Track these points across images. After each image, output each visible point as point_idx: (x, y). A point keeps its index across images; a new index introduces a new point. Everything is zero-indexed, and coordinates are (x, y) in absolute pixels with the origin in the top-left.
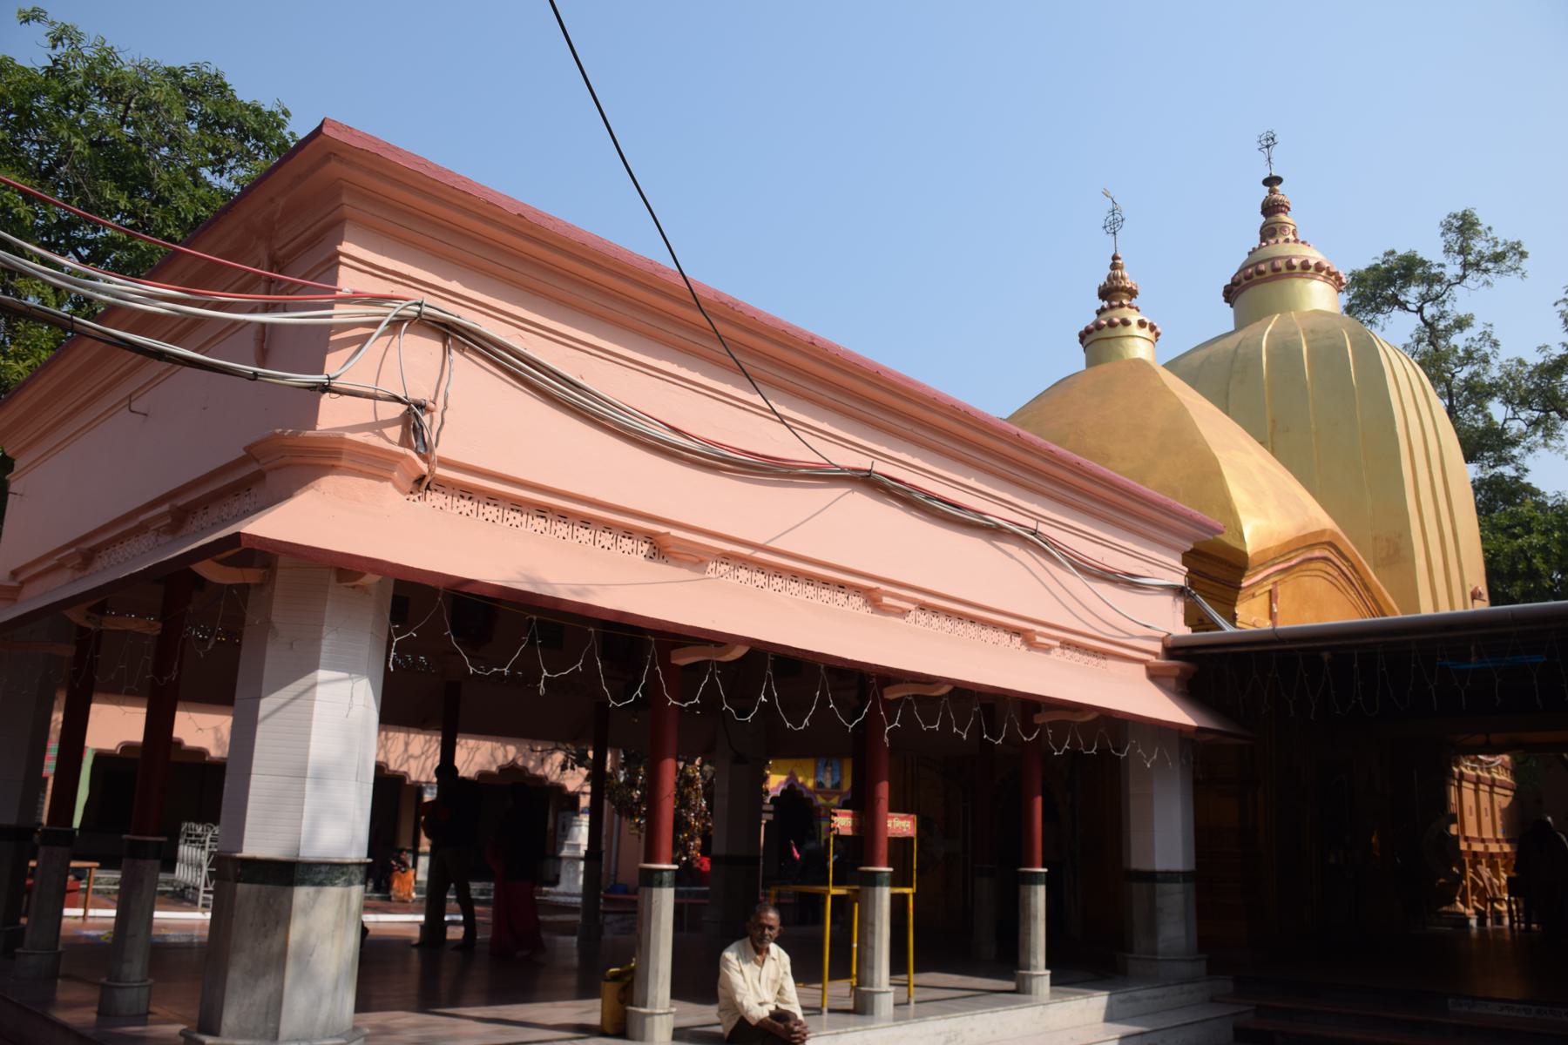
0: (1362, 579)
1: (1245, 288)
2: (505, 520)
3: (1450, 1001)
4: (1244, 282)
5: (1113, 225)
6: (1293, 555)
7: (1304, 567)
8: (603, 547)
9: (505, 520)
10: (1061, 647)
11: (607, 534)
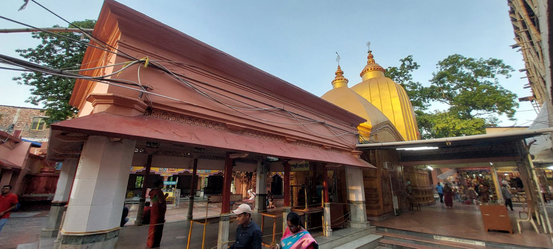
1: (365, 73)
2: (178, 120)
3: (434, 236)
4: (364, 72)
5: (338, 58)
6: (381, 126)
8: (209, 128)
9: (178, 120)
11: (211, 124)
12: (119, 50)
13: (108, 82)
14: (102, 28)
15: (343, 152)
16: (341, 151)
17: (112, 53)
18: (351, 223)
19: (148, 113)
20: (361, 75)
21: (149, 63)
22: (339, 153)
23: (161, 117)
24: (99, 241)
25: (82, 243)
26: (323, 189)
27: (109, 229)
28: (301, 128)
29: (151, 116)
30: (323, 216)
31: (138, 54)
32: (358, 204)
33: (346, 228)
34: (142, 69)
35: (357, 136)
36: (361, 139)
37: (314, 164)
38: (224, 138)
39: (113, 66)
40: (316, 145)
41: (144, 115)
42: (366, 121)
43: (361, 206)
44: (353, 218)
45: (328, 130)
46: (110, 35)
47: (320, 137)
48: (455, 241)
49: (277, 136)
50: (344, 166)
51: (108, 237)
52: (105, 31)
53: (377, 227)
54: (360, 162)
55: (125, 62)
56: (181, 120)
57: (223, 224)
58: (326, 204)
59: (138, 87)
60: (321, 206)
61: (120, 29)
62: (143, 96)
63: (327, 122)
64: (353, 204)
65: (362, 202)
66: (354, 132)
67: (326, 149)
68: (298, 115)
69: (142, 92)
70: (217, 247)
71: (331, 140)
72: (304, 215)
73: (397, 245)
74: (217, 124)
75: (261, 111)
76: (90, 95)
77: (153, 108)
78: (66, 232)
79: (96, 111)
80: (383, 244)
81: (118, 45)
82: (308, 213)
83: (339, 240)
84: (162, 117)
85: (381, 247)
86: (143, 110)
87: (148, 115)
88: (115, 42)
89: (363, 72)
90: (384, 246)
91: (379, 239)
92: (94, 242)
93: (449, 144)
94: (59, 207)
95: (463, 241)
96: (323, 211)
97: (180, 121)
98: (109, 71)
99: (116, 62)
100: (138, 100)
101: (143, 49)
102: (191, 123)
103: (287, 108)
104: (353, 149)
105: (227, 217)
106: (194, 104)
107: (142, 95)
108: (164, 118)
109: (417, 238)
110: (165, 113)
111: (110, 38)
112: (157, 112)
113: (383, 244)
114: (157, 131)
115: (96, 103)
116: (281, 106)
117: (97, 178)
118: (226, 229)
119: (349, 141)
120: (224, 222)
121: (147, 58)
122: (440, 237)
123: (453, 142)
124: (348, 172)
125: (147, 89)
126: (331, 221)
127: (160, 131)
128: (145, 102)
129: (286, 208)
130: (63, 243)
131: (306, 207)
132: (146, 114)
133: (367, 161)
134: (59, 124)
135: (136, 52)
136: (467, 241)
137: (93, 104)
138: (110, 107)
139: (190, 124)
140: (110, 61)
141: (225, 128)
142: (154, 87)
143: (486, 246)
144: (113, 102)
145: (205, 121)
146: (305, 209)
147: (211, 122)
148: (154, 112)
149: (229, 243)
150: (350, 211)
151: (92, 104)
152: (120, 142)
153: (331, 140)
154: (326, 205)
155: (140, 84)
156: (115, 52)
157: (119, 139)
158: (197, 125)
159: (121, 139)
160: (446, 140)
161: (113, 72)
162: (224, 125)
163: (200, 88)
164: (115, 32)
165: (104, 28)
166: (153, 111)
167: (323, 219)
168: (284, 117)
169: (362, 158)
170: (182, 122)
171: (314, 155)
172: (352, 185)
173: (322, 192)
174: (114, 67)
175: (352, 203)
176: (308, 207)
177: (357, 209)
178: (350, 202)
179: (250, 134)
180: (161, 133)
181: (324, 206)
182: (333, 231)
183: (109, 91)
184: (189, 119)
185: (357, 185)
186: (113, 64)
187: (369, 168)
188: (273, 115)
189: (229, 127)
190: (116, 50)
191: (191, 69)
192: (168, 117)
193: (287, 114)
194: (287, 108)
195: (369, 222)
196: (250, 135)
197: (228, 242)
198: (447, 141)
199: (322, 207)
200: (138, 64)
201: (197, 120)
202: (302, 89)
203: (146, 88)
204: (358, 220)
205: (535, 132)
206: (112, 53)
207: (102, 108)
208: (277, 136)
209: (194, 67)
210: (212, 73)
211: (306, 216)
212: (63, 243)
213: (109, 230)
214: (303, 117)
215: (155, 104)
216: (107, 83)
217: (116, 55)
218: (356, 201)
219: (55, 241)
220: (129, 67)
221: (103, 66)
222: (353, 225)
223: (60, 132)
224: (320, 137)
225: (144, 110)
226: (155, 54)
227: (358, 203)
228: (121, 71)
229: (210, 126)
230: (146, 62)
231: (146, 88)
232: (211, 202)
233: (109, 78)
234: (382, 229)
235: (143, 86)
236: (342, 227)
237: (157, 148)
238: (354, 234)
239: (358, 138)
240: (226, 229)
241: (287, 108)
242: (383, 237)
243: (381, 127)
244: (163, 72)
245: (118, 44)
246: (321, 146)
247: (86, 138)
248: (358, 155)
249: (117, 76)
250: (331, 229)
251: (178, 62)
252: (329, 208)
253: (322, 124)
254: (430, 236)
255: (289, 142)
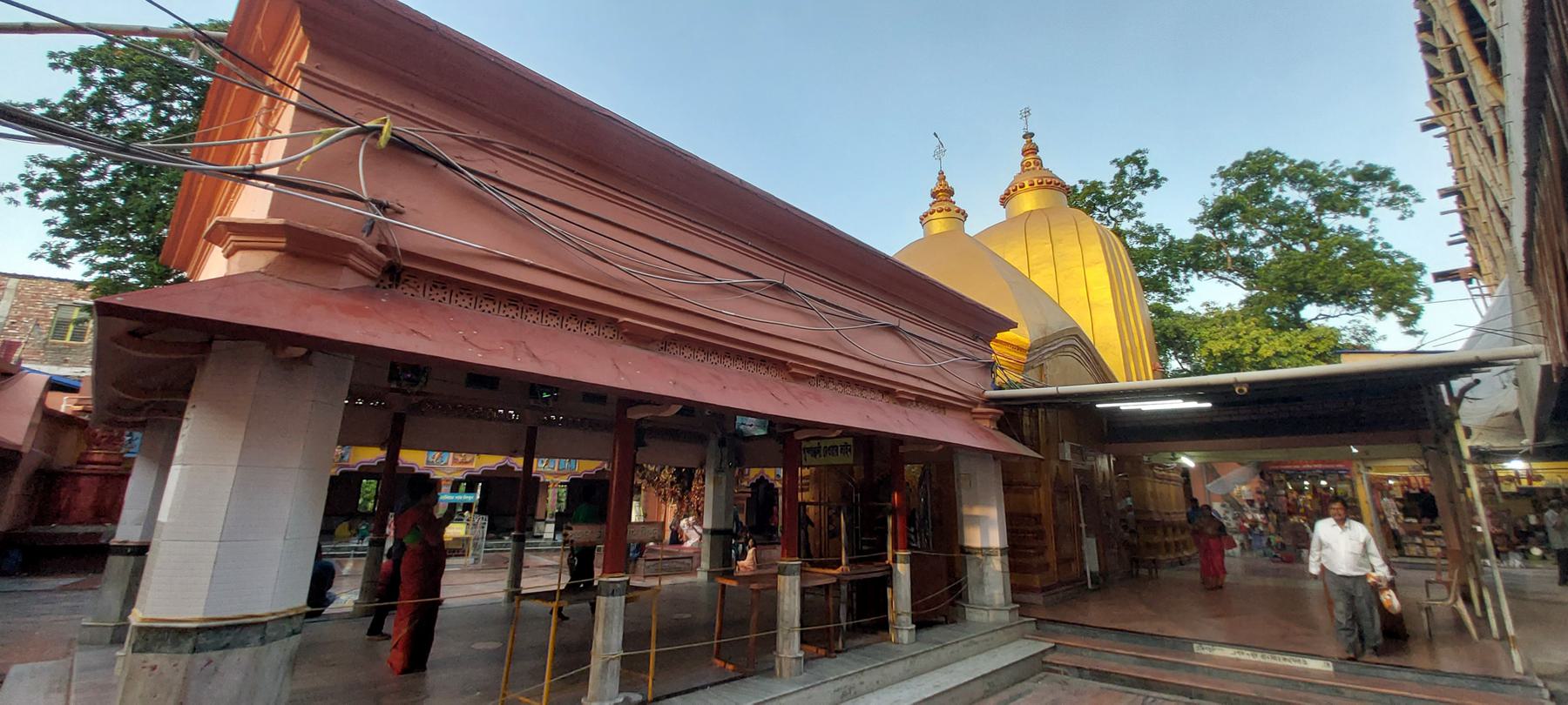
0: (1094, 358)
1: (1013, 196)
3: (1195, 646)
4: (1012, 193)
5: (940, 151)
6: (1056, 342)
7: (1062, 350)
8: (569, 330)
10: (917, 402)
12: (303, 91)
13: (272, 185)
14: (254, 29)
15: (948, 412)
16: (944, 408)
17: (285, 101)
18: (967, 609)
19: (391, 283)
20: (1004, 201)
21: (393, 134)
22: (938, 415)
23: (427, 294)
24: (244, 644)
25: (194, 650)
26: (893, 512)
27: (273, 611)
28: (832, 340)
29: (398, 291)
30: (892, 587)
31: (361, 109)
32: (988, 555)
33: (954, 622)
34: (372, 151)
35: (990, 367)
36: (1001, 377)
37: (866, 442)
38: (613, 360)
39: (286, 140)
40: (873, 388)
41: (378, 286)
42: (1013, 325)
43: (994, 561)
44: (973, 595)
45: (909, 347)
46: (280, 47)
47: (884, 367)
48: (1251, 658)
49: (763, 360)
50: (950, 448)
51: (270, 633)
52: (260, 37)
53: (1039, 621)
54: (996, 439)
55: (322, 130)
56: (487, 305)
57: (606, 604)
58: (900, 553)
59: (359, 202)
60: (887, 559)
61: (304, 30)
62: (374, 231)
63: (906, 326)
64: (973, 556)
65: (999, 552)
66: (982, 356)
67: (902, 402)
68: (823, 301)
69: (373, 218)
70: (589, 669)
71: (915, 377)
72: (837, 584)
73: (1090, 670)
74: (592, 319)
75: (719, 288)
76: (217, 221)
77: (405, 269)
78: (144, 617)
79: (235, 270)
80: (1055, 668)
81: (300, 79)
82: (848, 578)
83: (935, 654)
84: (430, 295)
85: (1044, 673)
86: (373, 270)
87: (390, 286)
88: (292, 70)
89: (1007, 194)
90: (1057, 672)
91: (1043, 652)
92: (227, 646)
93: (1240, 391)
94: (132, 558)
95: (1274, 658)
96: (891, 576)
97: (483, 308)
98: (275, 153)
99: (294, 127)
100: (358, 241)
101: (373, 95)
102: (517, 314)
103: (792, 282)
104: (975, 404)
105: (619, 585)
106: (526, 260)
107: (372, 227)
108: (440, 297)
109: (1146, 652)
110: (441, 283)
111: (277, 60)
112: (416, 280)
113: (1055, 668)
114: (413, 331)
115: (234, 246)
116: (777, 276)
117: (236, 464)
118: (616, 617)
119: (967, 382)
120: (611, 598)
121: (385, 121)
122: (1210, 647)
123: (1254, 385)
124: (963, 466)
125: (387, 210)
126: (912, 602)
127: (424, 333)
128: (380, 247)
129: (785, 563)
130: (137, 649)
131: (843, 561)
132: (382, 284)
133: (1016, 439)
134: (119, 299)
135: (353, 102)
136: (1285, 659)
137: (226, 252)
138: (277, 257)
139: (513, 317)
140: (277, 128)
141: (616, 333)
142: (407, 205)
143: (1336, 670)
144: (283, 245)
145: (557, 311)
146: (841, 568)
147: (574, 315)
148: (407, 280)
149: (622, 656)
150: (966, 574)
151: (221, 249)
152: (305, 359)
153: (915, 377)
154: (898, 557)
155: (365, 196)
156: (291, 100)
157: (302, 351)
158: (534, 322)
159: (309, 353)
160: (1235, 379)
161: (287, 154)
162: (612, 323)
163: (542, 214)
164: (291, 39)
165: (259, 28)
166: (403, 277)
167: (889, 596)
168: (780, 307)
169: (999, 430)
170: (489, 312)
171: (868, 417)
172: (971, 506)
173: (890, 521)
174: (288, 143)
175: (969, 553)
176: (851, 562)
177: (986, 570)
178: (967, 550)
179: (688, 353)
180: (428, 338)
181: (895, 559)
182: (916, 629)
183: (273, 212)
184: (510, 304)
185: (988, 505)
186: (287, 132)
187: (1021, 455)
188: (754, 299)
189: (626, 330)
190: (295, 92)
191: (516, 156)
192: (447, 296)
193: (793, 297)
194: (793, 282)
195: (1018, 606)
196: (685, 354)
197: (622, 654)
198: (1237, 383)
199: (887, 562)
200: (360, 137)
201: (534, 308)
202: (835, 229)
203: (383, 207)
204: (987, 601)
205: (1477, 357)
206: (285, 101)
207: (253, 261)
208: (763, 360)
209: (527, 153)
210: (578, 174)
211: (844, 587)
212: (137, 649)
213: (274, 614)
214: (837, 307)
215: (408, 254)
216: (265, 187)
217: (293, 106)
218: (981, 549)
219: (118, 653)
220: (332, 142)
221: (257, 138)
222: (974, 615)
223: (122, 324)
224: (884, 367)
225: (377, 273)
226: (409, 108)
227: (987, 552)
228: (310, 153)
229: (573, 325)
230: (385, 131)
231: (383, 207)
232: (572, 541)
233: (274, 172)
234: (1053, 627)
235: (373, 201)
236: (943, 619)
237: (418, 394)
238: (975, 639)
239: (993, 372)
240: (616, 617)
241: (792, 282)
242: (1054, 648)
243: (1055, 345)
244: (433, 162)
245: (300, 76)
246: (888, 392)
247: (205, 347)
248: (991, 419)
249: (298, 169)
250: (913, 623)
251: (479, 137)
252: (908, 565)
253: (892, 330)
254: (1183, 645)
255: (797, 378)
